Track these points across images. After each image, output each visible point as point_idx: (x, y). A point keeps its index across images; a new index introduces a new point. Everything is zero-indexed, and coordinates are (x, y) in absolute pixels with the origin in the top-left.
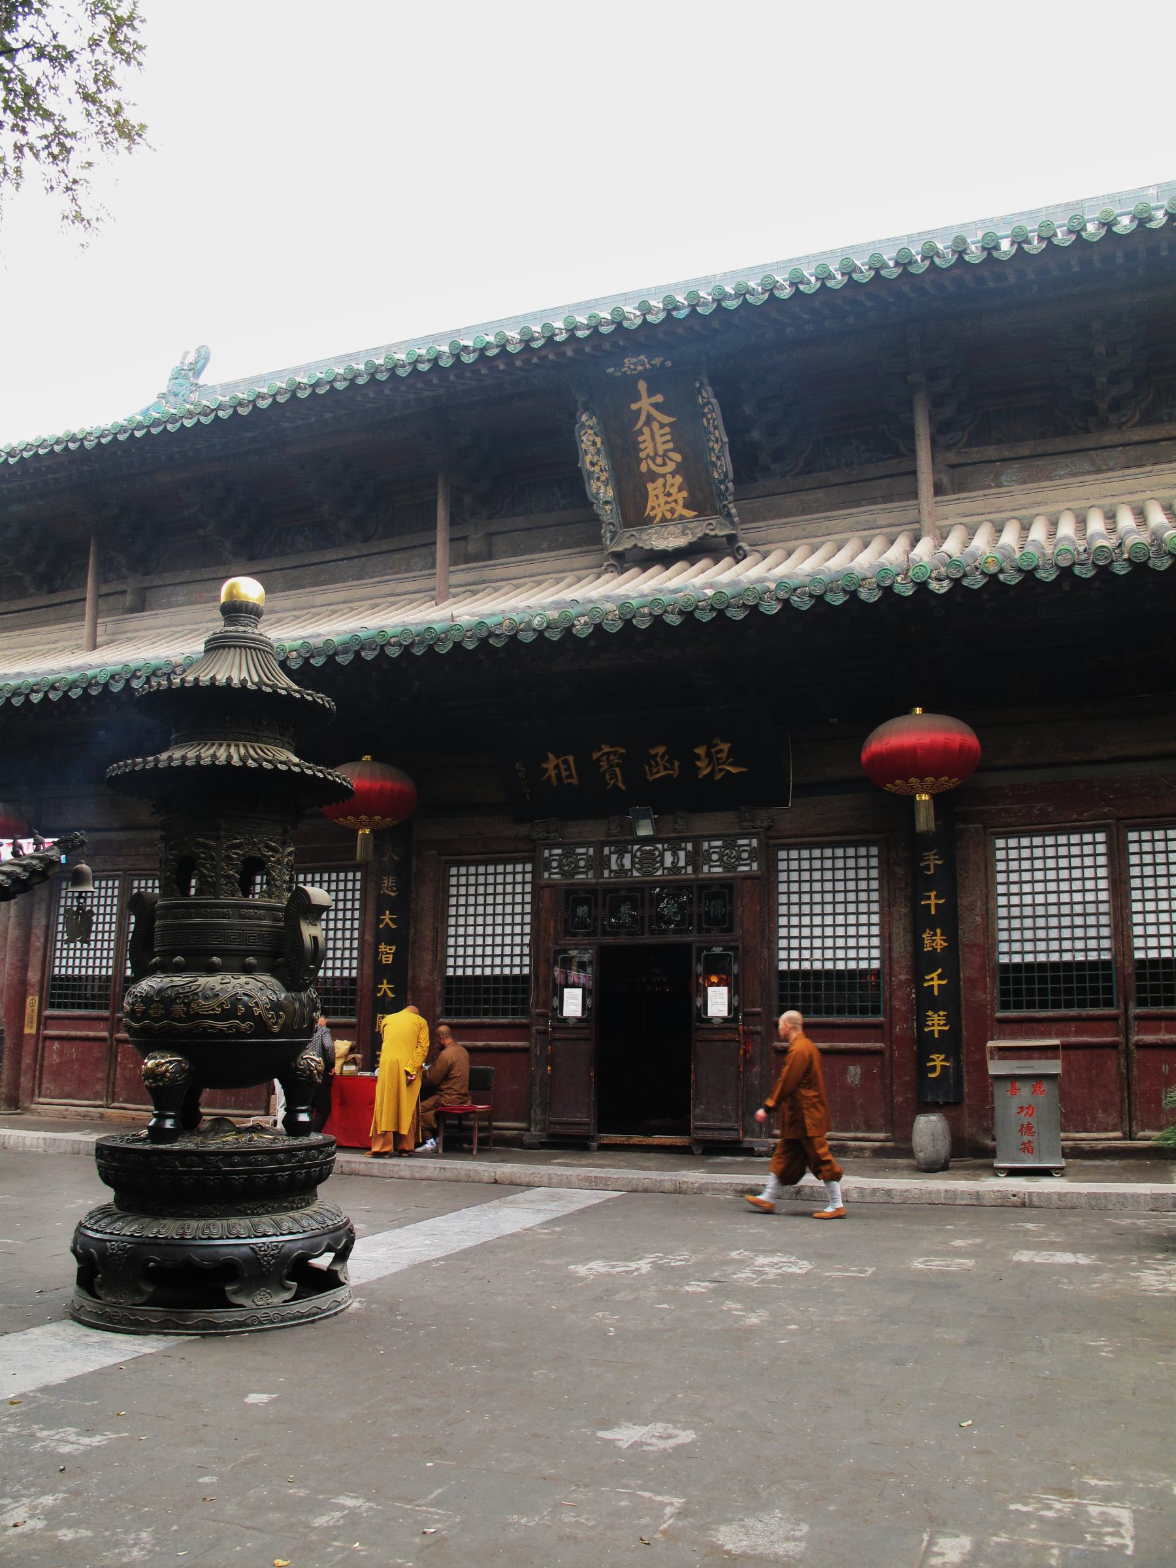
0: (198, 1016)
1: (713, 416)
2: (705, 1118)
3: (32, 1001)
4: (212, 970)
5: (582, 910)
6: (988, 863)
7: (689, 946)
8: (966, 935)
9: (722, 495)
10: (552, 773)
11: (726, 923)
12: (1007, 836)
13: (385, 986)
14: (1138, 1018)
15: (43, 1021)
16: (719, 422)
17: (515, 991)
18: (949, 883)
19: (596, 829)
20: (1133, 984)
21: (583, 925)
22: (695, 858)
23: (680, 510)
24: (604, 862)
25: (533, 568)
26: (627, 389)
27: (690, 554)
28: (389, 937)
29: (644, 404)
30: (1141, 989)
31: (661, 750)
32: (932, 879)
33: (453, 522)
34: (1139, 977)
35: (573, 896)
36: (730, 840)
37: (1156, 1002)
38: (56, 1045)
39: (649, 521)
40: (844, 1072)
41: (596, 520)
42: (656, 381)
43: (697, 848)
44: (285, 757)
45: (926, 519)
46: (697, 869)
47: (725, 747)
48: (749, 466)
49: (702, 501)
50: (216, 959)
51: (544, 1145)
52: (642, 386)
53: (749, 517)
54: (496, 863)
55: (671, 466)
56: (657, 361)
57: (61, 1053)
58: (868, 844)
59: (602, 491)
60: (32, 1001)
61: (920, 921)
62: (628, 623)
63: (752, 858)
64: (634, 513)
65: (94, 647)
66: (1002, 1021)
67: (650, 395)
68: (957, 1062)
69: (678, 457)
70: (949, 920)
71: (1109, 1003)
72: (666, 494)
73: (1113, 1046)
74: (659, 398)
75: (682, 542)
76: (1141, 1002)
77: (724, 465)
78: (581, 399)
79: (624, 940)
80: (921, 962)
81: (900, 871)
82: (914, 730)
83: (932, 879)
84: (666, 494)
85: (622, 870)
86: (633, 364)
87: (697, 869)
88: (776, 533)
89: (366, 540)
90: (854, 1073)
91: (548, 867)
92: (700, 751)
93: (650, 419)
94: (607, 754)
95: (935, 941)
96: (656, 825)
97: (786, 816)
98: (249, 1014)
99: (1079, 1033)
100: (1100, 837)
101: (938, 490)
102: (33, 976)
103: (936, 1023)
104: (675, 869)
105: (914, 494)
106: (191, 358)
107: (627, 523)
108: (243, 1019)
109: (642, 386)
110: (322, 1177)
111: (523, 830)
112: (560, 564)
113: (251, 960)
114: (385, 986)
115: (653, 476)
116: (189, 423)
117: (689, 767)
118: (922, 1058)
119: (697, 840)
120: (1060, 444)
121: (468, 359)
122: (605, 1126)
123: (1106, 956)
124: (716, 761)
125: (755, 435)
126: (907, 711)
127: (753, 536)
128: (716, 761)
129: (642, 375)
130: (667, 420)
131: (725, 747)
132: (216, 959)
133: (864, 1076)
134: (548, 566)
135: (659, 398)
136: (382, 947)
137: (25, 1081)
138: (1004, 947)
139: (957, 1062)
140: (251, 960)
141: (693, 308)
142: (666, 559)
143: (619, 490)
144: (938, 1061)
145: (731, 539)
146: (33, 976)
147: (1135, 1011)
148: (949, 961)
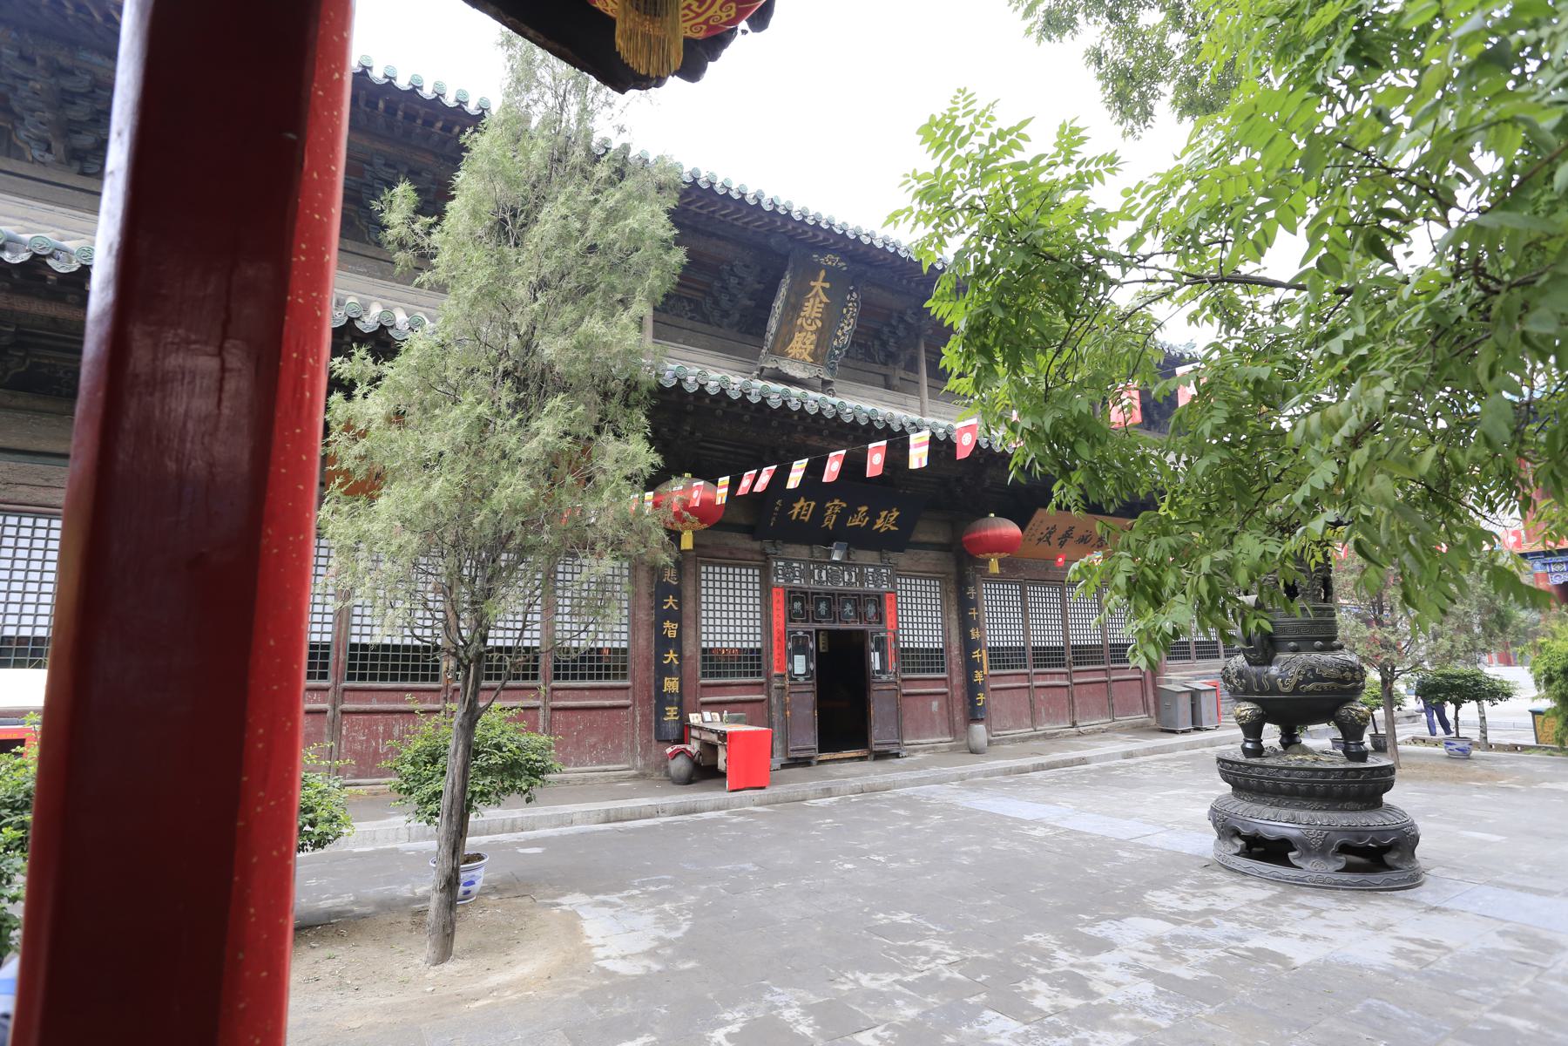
1: (851, 311)
2: (879, 736)
7: (862, 633)
9: (832, 355)
10: (796, 511)
11: (880, 618)
13: (672, 655)
17: (752, 659)
19: (803, 551)
21: (797, 614)
22: (861, 578)
23: (805, 356)
28: (676, 617)
29: (818, 285)
31: (865, 509)
42: (832, 274)
43: (861, 571)
49: (819, 355)
51: (783, 766)
52: (823, 274)
55: (814, 327)
58: (935, 579)
59: (773, 324)
69: (819, 324)
72: (803, 343)
74: (827, 285)
78: (791, 265)
84: (803, 343)
85: (820, 582)
86: (830, 260)
87: (862, 585)
91: (776, 574)
97: (903, 559)
104: (849, 583)
109: (823, 274)
111: (757, 545)
114: (672, 655)
115: (802, 329)
119: (861, 566)
122: (823, 748)
128: (886, 521)
130: (825, 300)
131: (896, 514)
133: (940, 707)
135: (827, 285)
136: (667, 624)
144: (981, 696)
148: (678, 643)
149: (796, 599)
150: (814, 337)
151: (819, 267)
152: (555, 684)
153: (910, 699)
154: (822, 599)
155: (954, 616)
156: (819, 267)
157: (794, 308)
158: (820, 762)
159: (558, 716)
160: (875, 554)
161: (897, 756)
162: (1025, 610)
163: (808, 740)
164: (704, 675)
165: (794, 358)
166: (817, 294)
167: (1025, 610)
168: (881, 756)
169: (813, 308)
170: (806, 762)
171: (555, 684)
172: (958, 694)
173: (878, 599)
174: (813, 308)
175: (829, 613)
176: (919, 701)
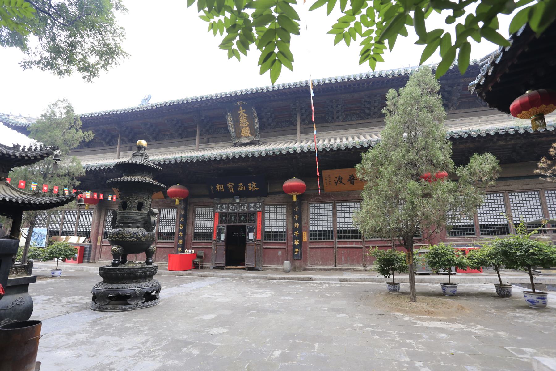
0: (125, 237)
1: (255, 115)
2: (249, 262)
3: (100, 237)
4: (129, 227)
5: (224, 218)
6: (308, 210)
7: (245, 226)
8: (303, 224)
9: (257, 131)
11: (254, 221)
12: (312, 204)
14: (338, 242)
15: (102, 242)
16: (257, 116)
18: (300, 213)
19: (228, 201)
20: (337, 235)
21: (224, 221)
22: (248, 207)
23: (248, 134)
24: (229, 208)
25: (217, 145)
26: (237, 108)
27: (250, 144)
29: (241, 112)
30: (338, 236)
31: (241, 184)
32: (297, 212)
33: (201, 135)
34: (338, 233)
35: (222, 215)
36: (255, 203)
37: (341, 239)
38: (105, 247)
39: (242, 136)
40: (278, 253)
41: (231, 136)
42: (244, 107)
43: (248, 205)
44: (150, 180)
45: (298, 138)
46: (248, 209)
47: (255, 184)
48: (263, 127)
49: (253, 133)
50: (130, 225)
51: (214, 268)
52: (241, 108)
53: (262, 137)
54: (206, 207)
55: (246, 125)
56: (244, 103)
57: (106, 249)
58: (284, 205)
59: (232, 129)
60: (100, 237)
61: (294, 221)
62: (234, 157)
63: (260, 207)
64: (238, 135)
65: (119, 158)
66: (310, 242)
67: (243, 109)
68: (301, 250)
70: (300, 221)
71: (332, 239)
72: (246, 131)
73: (333, 247)
74: (244, 111)
75: (248, 141)
76: (338, 239)
77: (257, 125)
79: (232, 224)
80: (294, 230)
81: (290, 211)
82: (293, 182)
83: (297, 212)
84: (246, 131)
85: (232, 210)
87: (248, 209)
88: (268, 140)
89: (182, 138)
90: (280, 253)
91: (217, 209)
92: (250, 184)
93: (242, 115)
94: (230, 185)
95: (297, 225)
96: (240, 200)
97: (267, 199)
98: (137, 237)
99: (326, 245)
100: (331, 204)
101: (301, 133)
102: (100, 232)
103: (297, 242)
104: (244, 209)
105: (296, 134)
106: (147, 97)
107: (237, 137)
108: (136, 238)
109: (241, 108)
110: (153, 274)
111: (212, 200)
112: (222, 145)
113: (139, 225)
115: (243, 127)
116: (141, 110)
117: (247, 188)
118: (294, 250)
119: (249, 203)
120: (326, 124)
121: (204, 99)
123: (332, 229)
124: (253, 186)
125: (265, 120)
126: (292, 177)
127: (264, 141)
128: (253, 186)
129: (241, 105)
130: (246, 115)
131: (255, 184)
132: (130, 225)
133: (282, 253)
134: (220, 145)
135: (244, 111)
137: (97, 256)
138: (311, 227)
139: (301, 250)
140: (139, 225)
141: (252, 92)
142: (245, 144)
143: (235, 129)
144: (297, 250)
145: (258, 141)
146: (100, 232)
147: (337, 240)
149: (223, 216)
150: (248, 128)
151: (239, 106)
152: (158, 241)
153: (267, 250)
154: (233, 216)
155: (290, 219)
156: (239, 106)
157: (236, 122)
158: (227, 269)
159: (158, 249)
160: (256, 199)
161: (257, 270)
162: (334, 214)
163: (223, 261)
164: (194, 240)
165: (245, 136)
166: (242, 115)
167: (334, 214)
168: (250, 269)
169: (243, 119)
170: (221, 268)
171: (158, 241)
172: (290, 249)
173: (254, 214)
174: (243, 119)
175: (235, 220)
176: (271, 251)
